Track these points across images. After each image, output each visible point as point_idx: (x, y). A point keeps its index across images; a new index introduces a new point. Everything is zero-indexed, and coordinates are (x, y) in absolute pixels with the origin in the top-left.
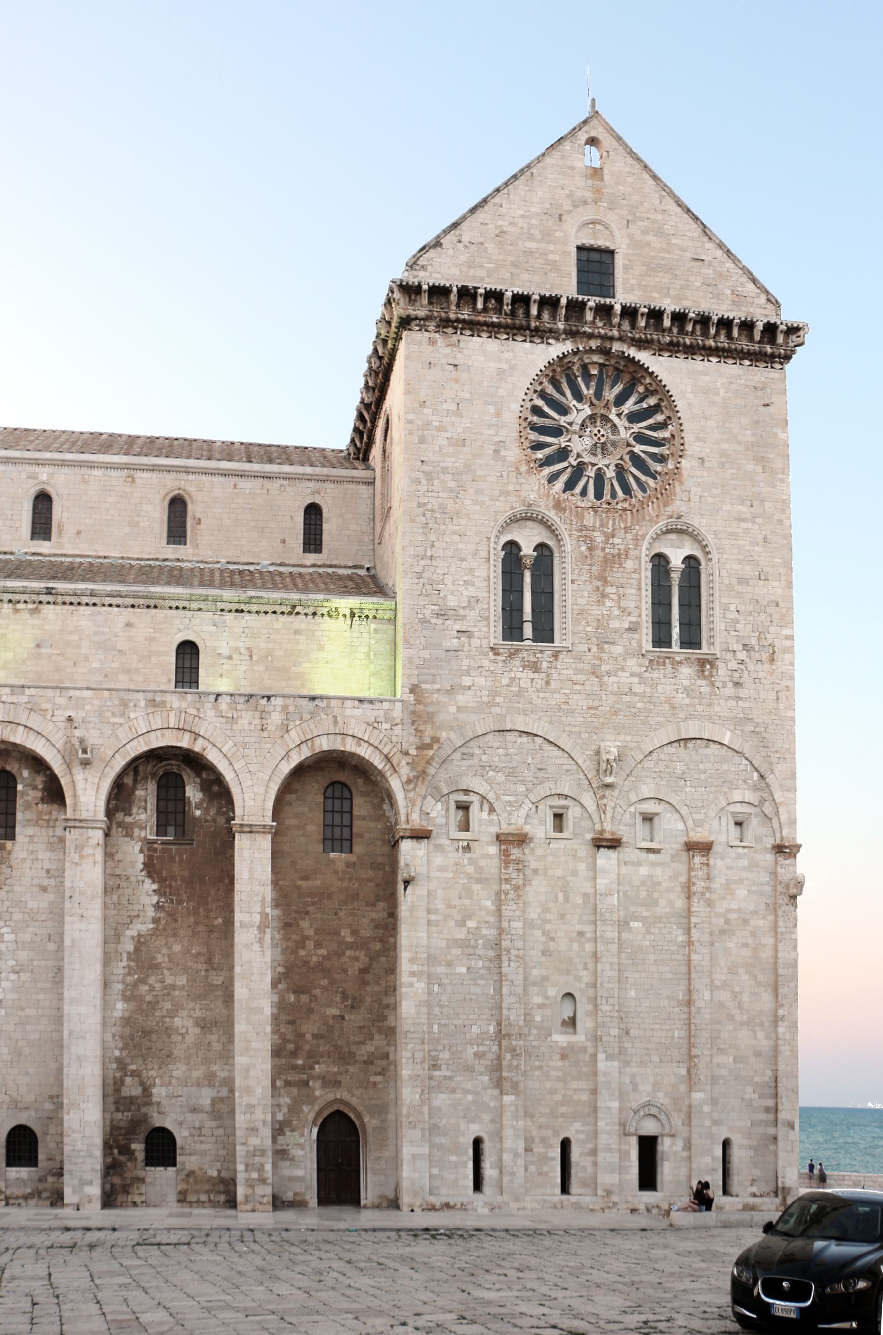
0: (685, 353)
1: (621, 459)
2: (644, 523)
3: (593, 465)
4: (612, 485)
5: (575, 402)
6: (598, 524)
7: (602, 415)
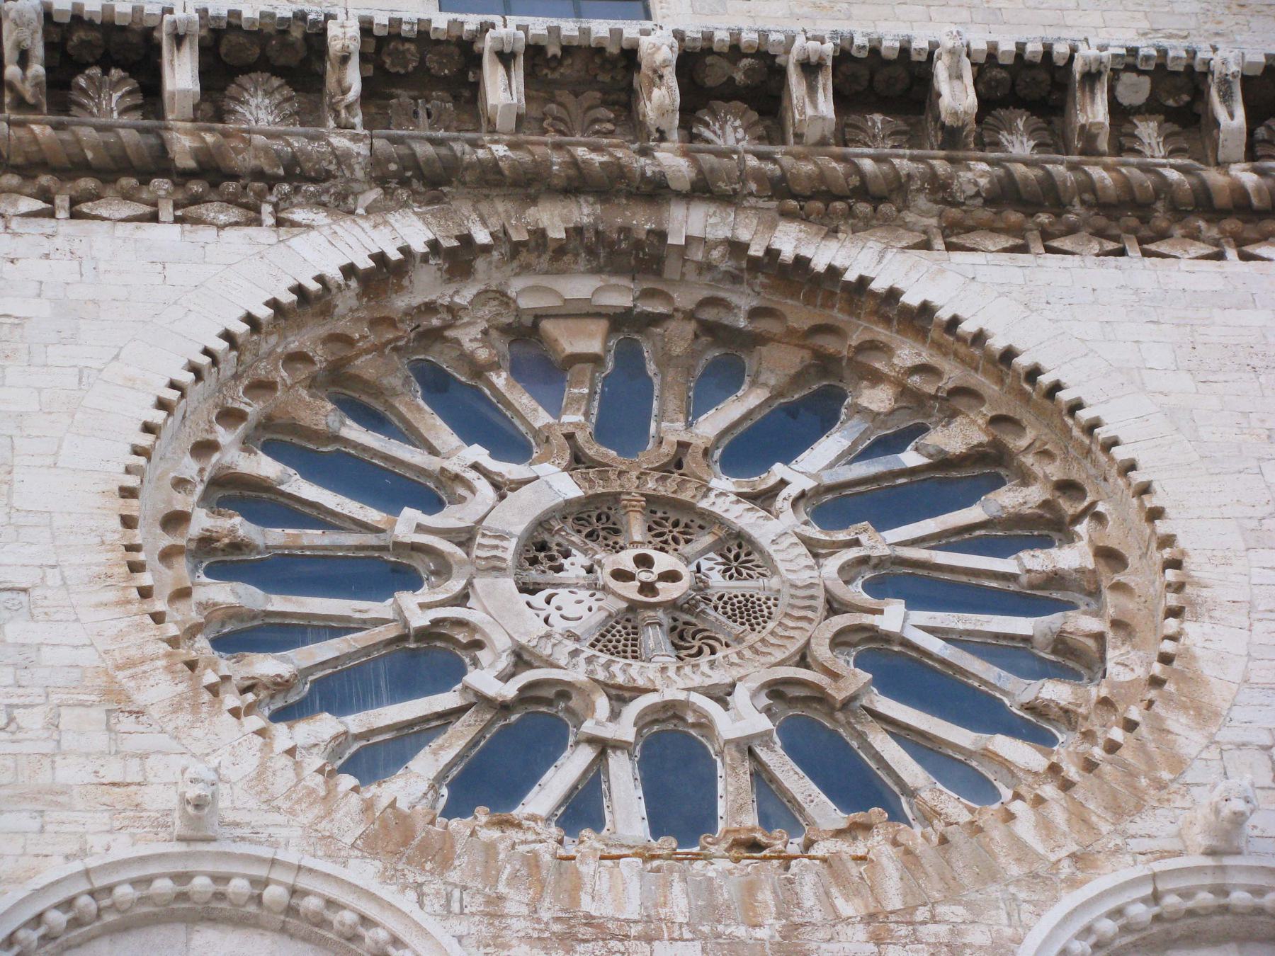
0: (1100, 234)
1: (803, 659)
2: (994, 891)
3: (620, 695)
4: (762, 779)
5: (478, 453)
6: (679, 904)
7: (652, 501)
